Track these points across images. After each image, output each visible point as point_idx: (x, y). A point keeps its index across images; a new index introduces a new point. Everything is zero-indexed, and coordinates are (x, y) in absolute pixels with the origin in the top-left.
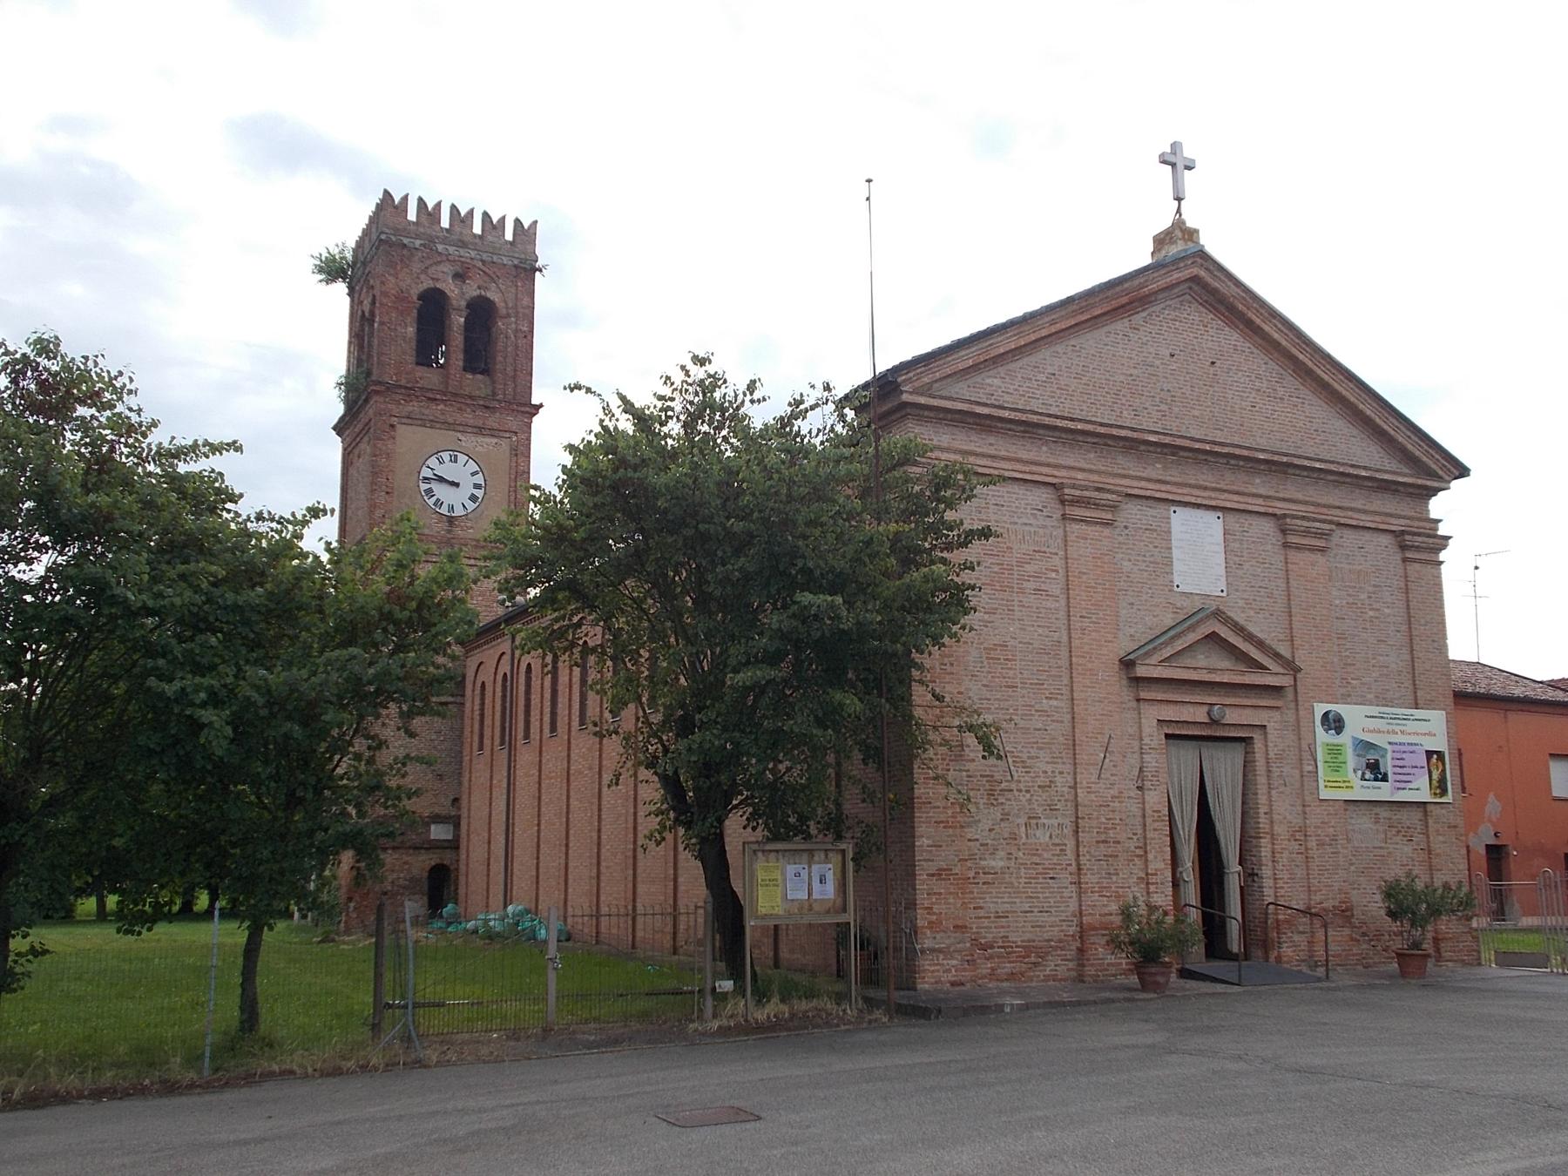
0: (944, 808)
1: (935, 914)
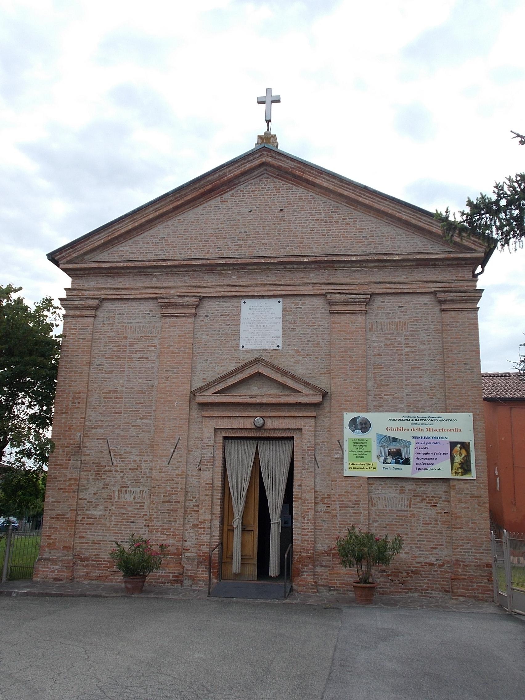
0: (64, 481)
1: (52, 539)
